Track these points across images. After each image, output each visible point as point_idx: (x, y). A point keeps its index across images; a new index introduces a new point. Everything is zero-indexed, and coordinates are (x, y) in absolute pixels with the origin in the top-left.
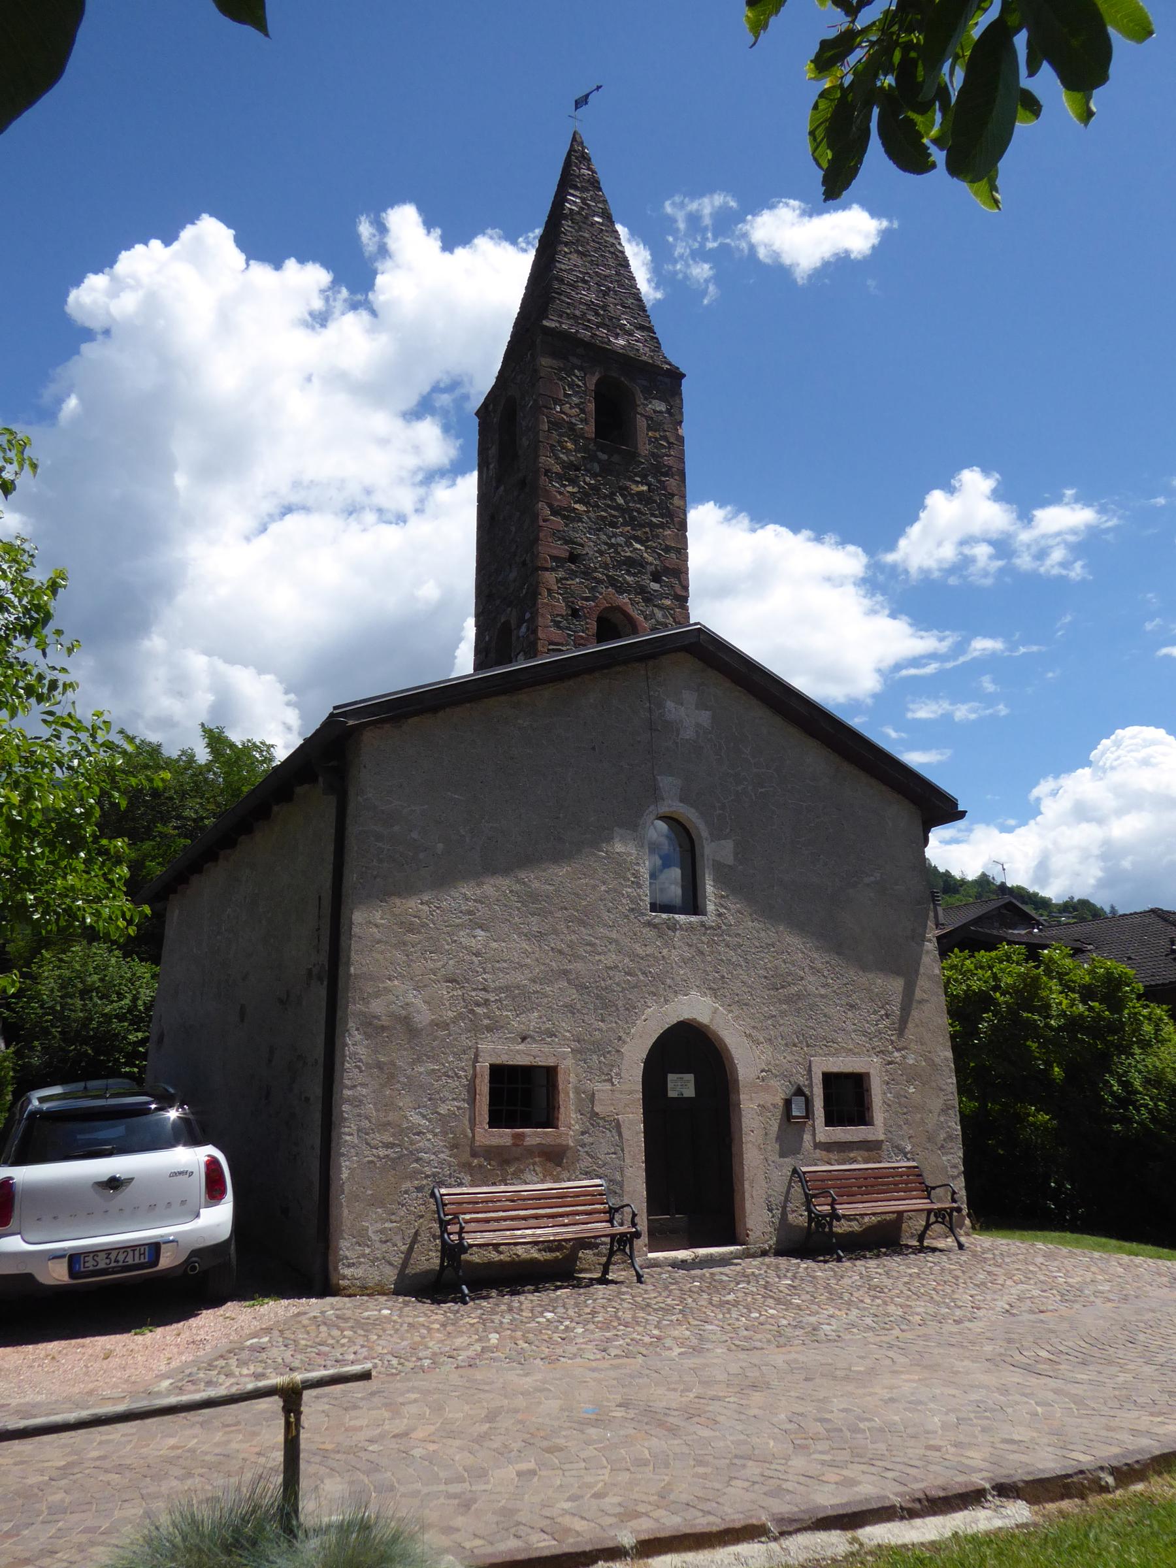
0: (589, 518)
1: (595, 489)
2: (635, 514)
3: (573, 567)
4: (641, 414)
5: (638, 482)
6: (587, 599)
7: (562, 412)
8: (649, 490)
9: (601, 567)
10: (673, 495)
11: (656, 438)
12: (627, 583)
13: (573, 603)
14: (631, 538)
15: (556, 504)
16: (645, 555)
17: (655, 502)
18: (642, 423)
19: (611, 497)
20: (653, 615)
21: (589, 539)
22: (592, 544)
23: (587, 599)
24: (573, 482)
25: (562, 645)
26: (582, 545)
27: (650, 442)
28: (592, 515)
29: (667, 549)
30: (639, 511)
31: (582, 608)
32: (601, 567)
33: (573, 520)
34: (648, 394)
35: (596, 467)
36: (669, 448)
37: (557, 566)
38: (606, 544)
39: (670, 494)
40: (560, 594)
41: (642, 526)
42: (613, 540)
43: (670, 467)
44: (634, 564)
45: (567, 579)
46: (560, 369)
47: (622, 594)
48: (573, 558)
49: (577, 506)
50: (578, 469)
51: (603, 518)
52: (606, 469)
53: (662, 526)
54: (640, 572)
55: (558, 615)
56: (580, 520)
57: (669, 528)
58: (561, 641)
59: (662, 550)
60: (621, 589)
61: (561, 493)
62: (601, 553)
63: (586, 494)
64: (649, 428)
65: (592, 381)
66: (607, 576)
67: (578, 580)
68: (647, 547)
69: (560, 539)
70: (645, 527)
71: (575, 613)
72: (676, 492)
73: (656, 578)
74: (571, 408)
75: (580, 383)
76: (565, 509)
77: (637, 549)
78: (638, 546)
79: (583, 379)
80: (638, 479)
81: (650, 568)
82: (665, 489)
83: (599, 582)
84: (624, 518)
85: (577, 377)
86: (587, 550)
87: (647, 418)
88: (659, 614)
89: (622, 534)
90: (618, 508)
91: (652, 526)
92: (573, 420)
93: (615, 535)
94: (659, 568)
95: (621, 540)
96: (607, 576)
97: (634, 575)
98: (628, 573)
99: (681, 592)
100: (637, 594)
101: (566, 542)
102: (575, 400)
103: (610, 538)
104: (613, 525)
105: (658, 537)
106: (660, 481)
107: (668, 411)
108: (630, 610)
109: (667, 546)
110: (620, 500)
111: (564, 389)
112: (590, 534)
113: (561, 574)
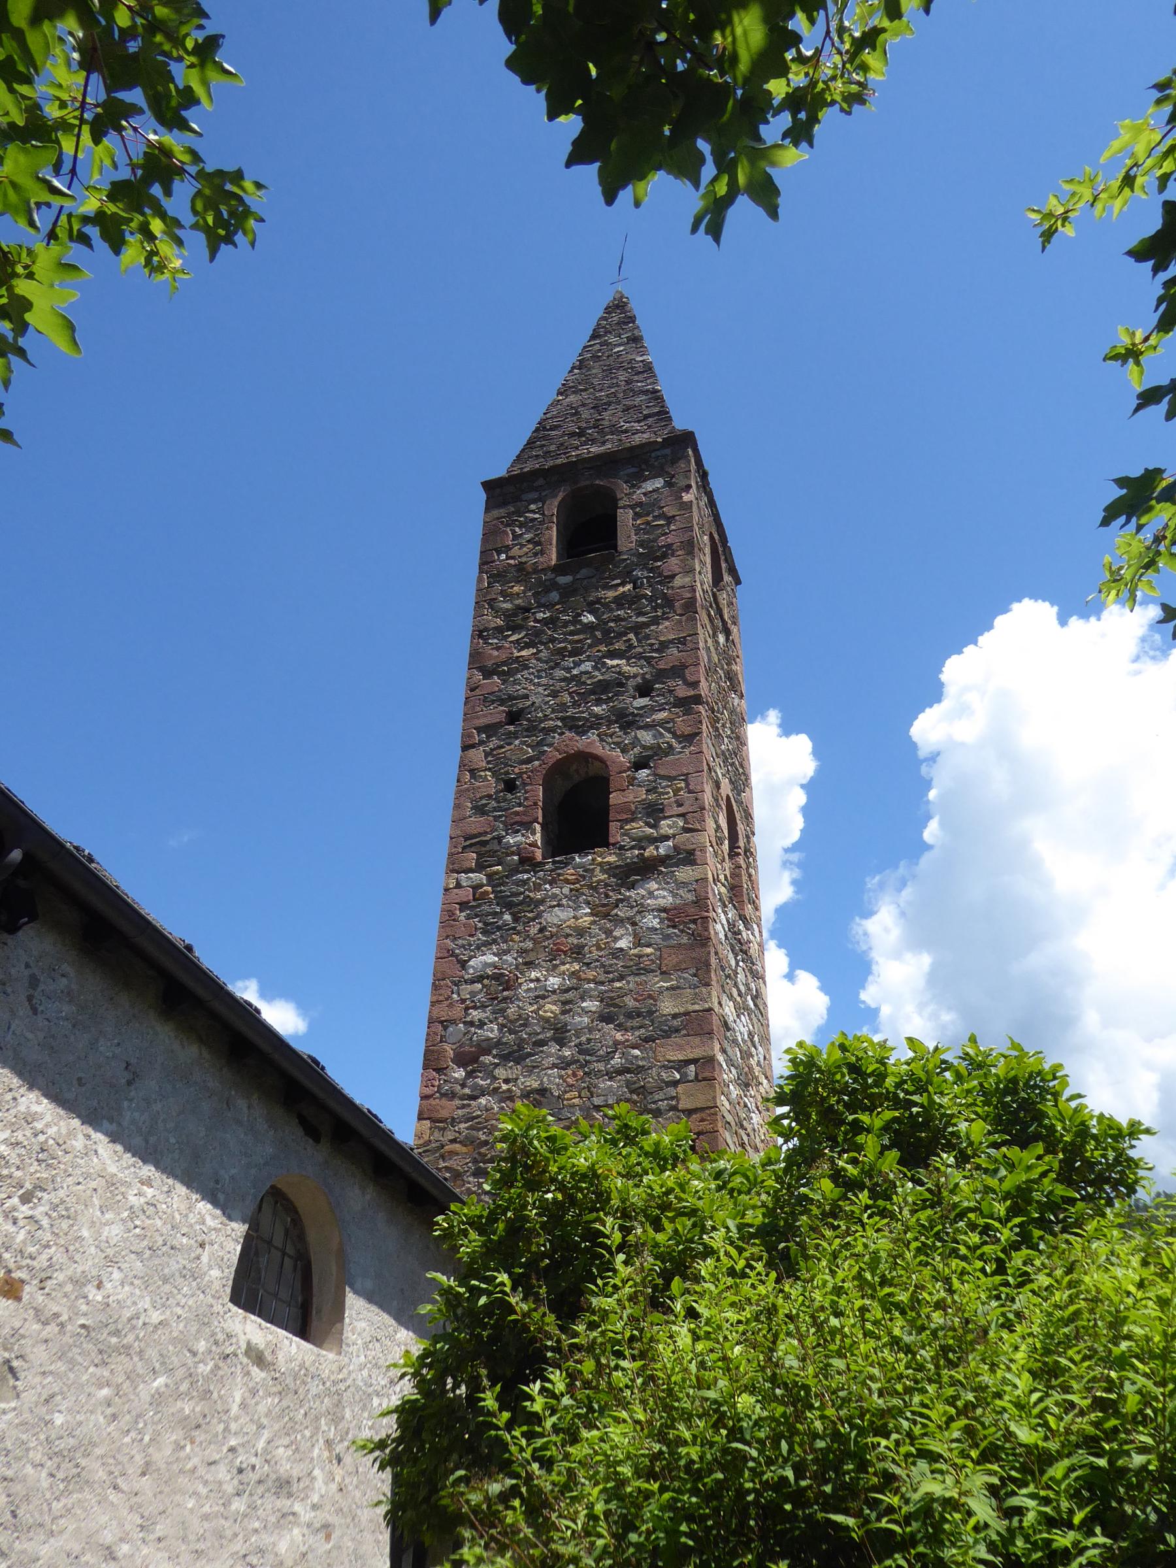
0: (538, 659)
1: (551, 622)
2: (612, 624)
3: (511, 728)
4: (624, 507)
5: (618, 585)
6: (529, 760)
7: (508, 558)
8: (634, 588)
9: (553, 711)
10: (673, 576)
11: (648, 523)
12: (597, 716)
13: (507, 773)
14: (604, 657)
15: (489, 663)
16: (626, 669)
17: (645, 596)
18: (625, 518)
19: (576, 620)
20: (636, 742)
21: (539, 685)
22: (540, 689)
23: (529, 760)
24: (515, 629)
25: (486, 833)
26: (526, 697)
27: (638, 530)
28: (544, 654)
29: (664, 646)
30: (618, 619)
31: (520, 774)
32: (553, 712)
33: (511, 673)
34: (637, 479)
35: (555, 596)
36: (668, 524)
37: (488, 737)
38: (564, 679)
39: (666, 577)
40: (489, 770)
41: (620, 635)
42: (575, 672)
43: (669, 546)
44: (604, 689)
45: (502, 747)
46: (509, 515)
47: (584, 733)
48: (513, 717)
49: (524, 653)
50: (527, 610)
51: (561, 652)
52: (567, 592)
53: (656, 621)
54: (617, 694)
55: (481, 798)
56: (527, 667)
57: (667, 619)
58: (481, 830)
59: (656, 651)
60: (578, 726)
61: (498, 648)
62: (554, 694)
63: (538, 633)
64: (637, 516)
65: (553, 507)
66: (562, 719)
67: (517, 742)
68: (628, 659)
69: (493, 702)
70: (626, 634)
71: (510, 786)
72: (677, 570)
73: (644, 690)
74: (522, 546)
75: (537, 516)
76: (504, 663)
77: (613, 667)
78: (615, 662)
79: (540, 511)
80: (619, 581)
81: (631, 683)
82: (660, 575)
83: (553, 730)
84: (594, 637)
85: (533, 512)
86: (533, 698)
87: (632, 507)
88: (646, 737)
89: (589, 659)
90: (590, 628)
91: (637, 629)
92: (524, 560)
93: (577, 664)
94: (647, 676)
95: (587, 666)
96: (562, 719)
97: (606, 702)
98: (598, 702)
99: (683, 691)
100: (610, 724)
101: (502, 702)
102: (528, 536)
103: (568, 670)
104: (575, 653)
105: (647, 637)
106: (651, 570)
107: (669, 484)
108: (599, 749)
109: (661, 643)
110: (589, 618)
111: (514, 532)
112: (539, 677)
113: (494, 742)
